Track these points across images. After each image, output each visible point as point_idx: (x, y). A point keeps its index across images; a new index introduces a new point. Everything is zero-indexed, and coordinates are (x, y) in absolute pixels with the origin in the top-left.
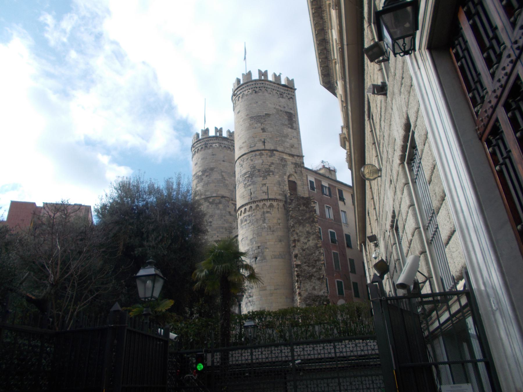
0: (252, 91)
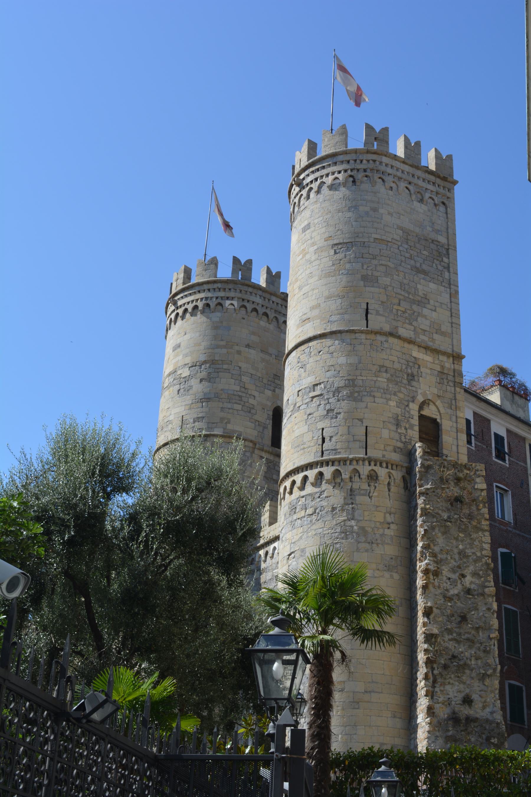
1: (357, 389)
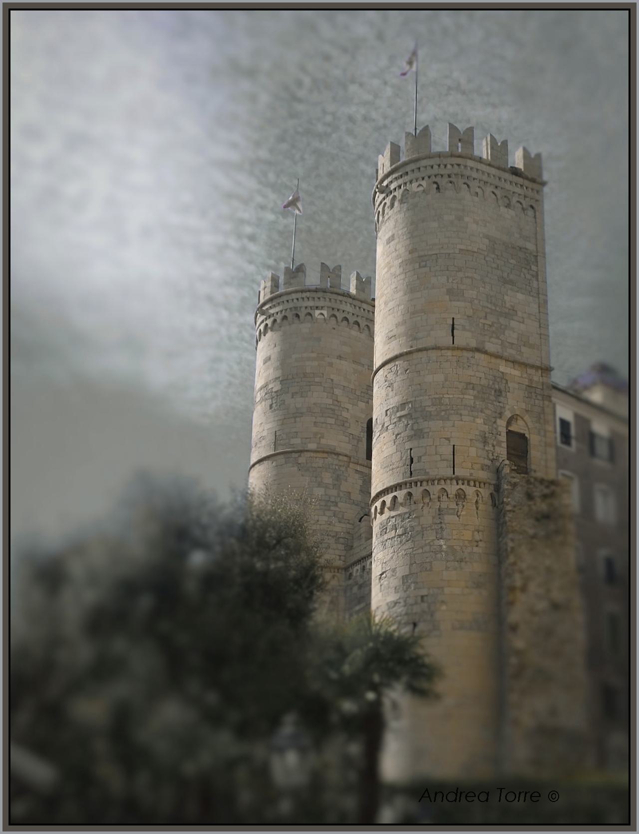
1: (443, 407)
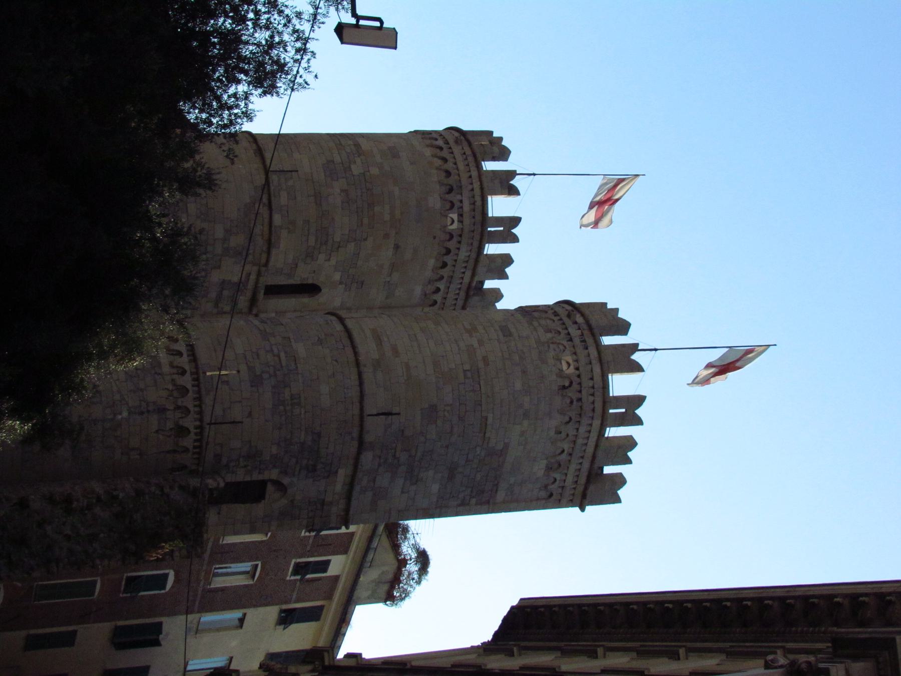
0: (568, 377)
1: (288, 408)
